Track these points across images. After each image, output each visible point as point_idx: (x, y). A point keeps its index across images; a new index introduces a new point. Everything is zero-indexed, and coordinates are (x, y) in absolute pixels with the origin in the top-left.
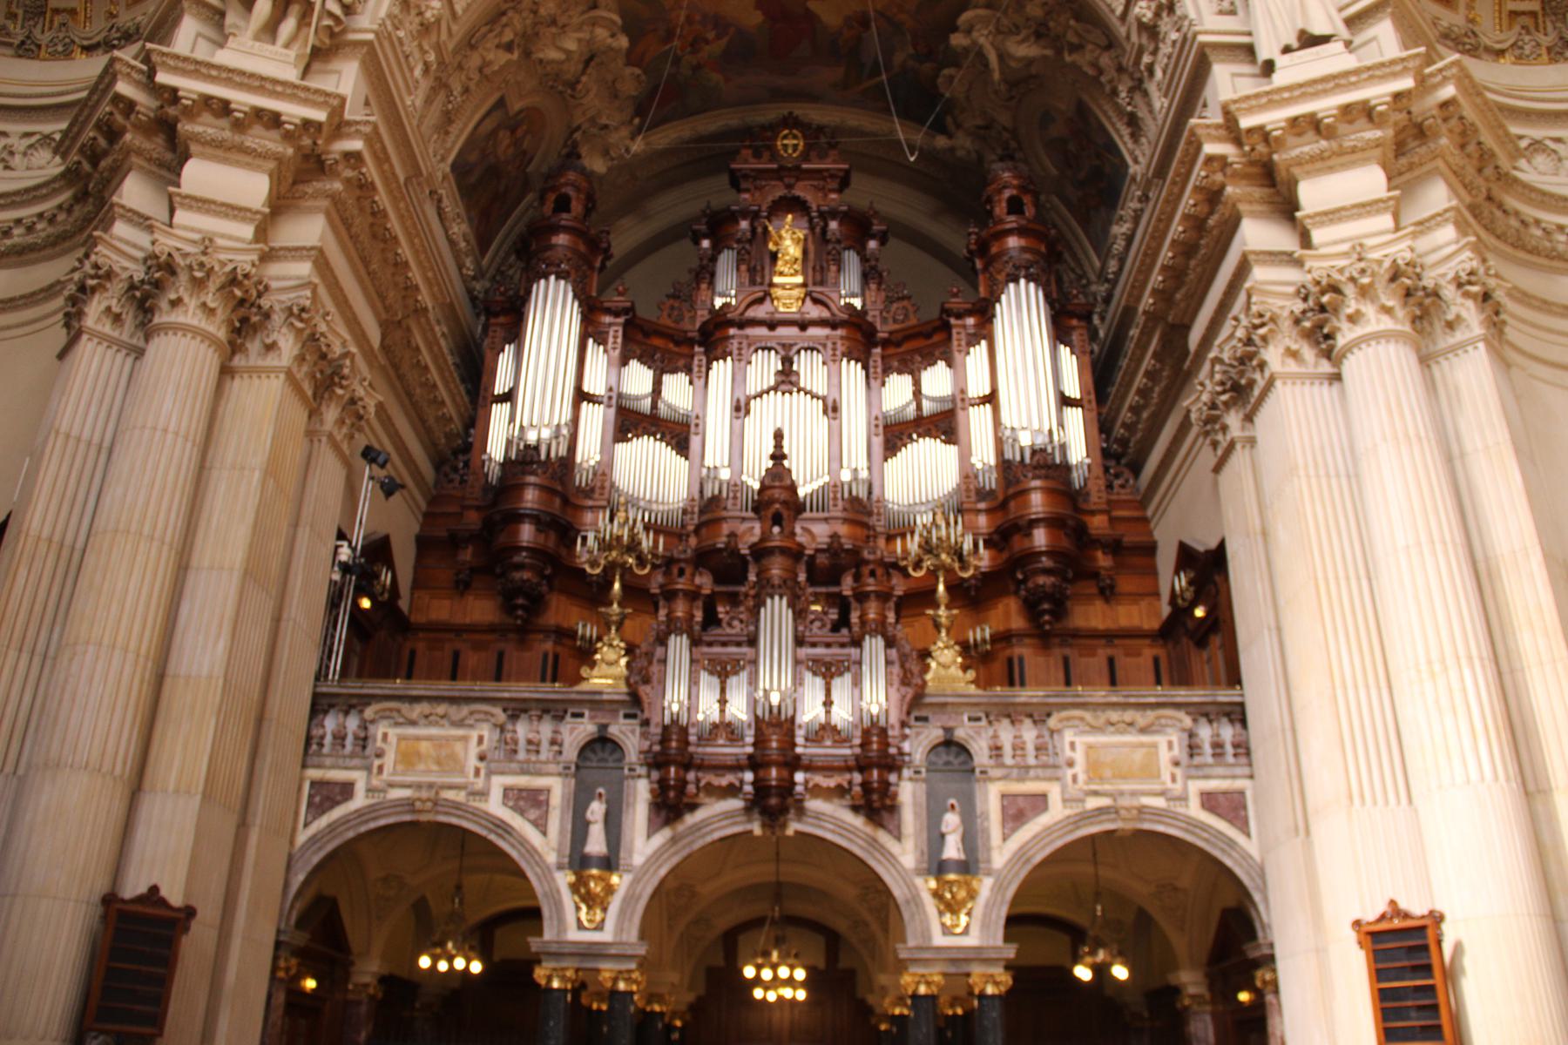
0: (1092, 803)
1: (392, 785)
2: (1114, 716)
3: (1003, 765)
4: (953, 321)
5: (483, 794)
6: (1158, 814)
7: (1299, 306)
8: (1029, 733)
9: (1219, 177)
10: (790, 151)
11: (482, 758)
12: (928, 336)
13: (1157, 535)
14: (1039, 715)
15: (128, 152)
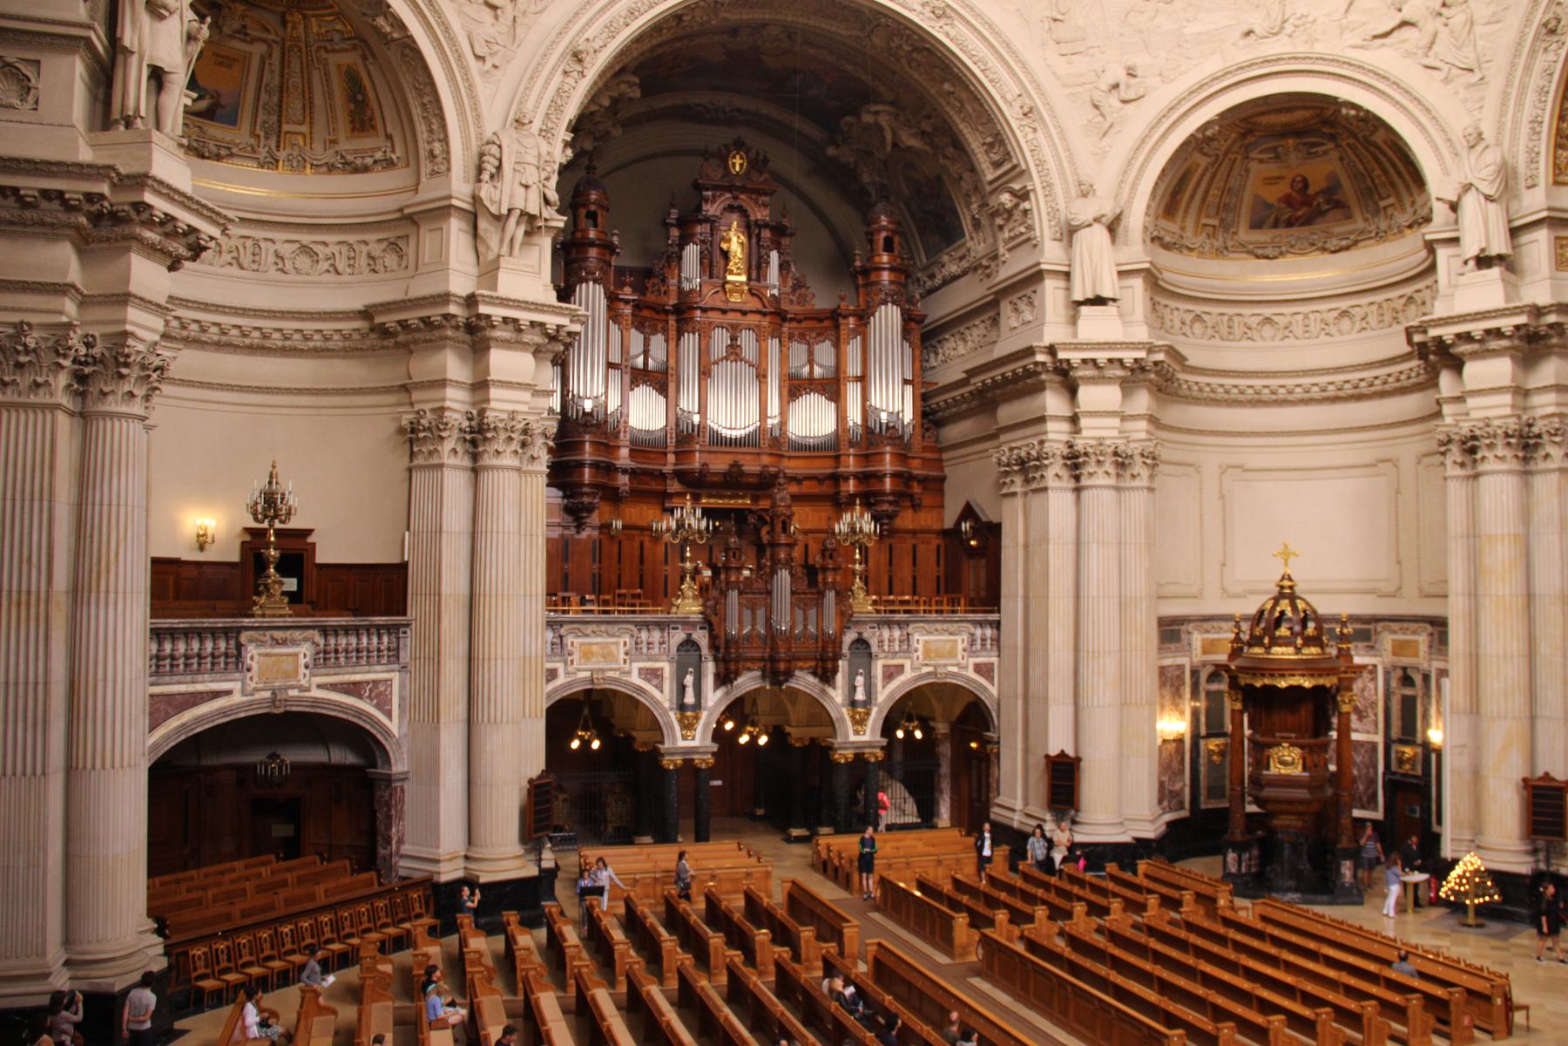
0: (925, 670)
1: (579, 670)
2: (939, 626)
3: (884, 651)
4: (841, 321)
5: (629, 673)
6: (954, 675)
7: (1066, 451)
8: (897, 633)
9: (1039, 369)
10: (738, 169)
11: (626, 654)
12: (821, 321)
13: (947, 471)
14: (900, 624)
15: (447, 338)
